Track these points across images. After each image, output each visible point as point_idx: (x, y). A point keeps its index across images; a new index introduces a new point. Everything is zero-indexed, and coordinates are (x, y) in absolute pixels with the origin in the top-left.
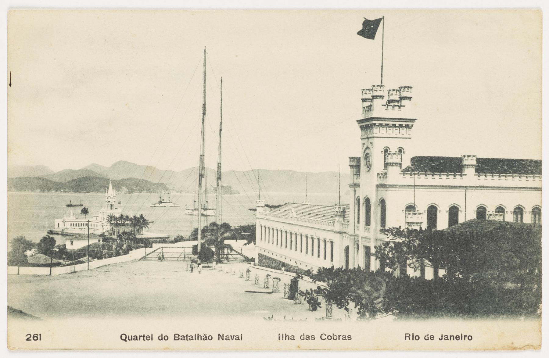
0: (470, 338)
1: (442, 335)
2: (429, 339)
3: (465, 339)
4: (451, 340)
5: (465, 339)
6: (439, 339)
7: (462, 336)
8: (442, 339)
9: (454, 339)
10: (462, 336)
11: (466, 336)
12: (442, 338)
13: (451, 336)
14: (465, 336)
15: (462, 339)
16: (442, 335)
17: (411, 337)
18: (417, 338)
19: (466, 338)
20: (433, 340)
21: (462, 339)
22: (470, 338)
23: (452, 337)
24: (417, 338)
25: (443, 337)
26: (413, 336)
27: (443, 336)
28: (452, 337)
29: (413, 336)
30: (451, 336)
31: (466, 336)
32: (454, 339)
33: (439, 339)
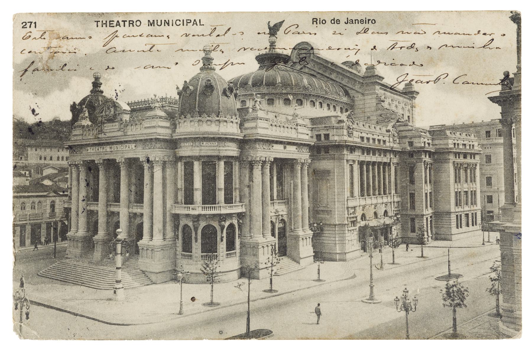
0: (373, 22)
1: (347, 18)
2: (335, 23)
3: (368, 23)
4: (355, 23)
5: (368, 23)
6: (345, 22)
7: (366, 20)
8: (348, 23)
9: (358, 23)
10: (366, 20)
11: (370, 20)
12: (348, 21)
13: (355, 20)
14: (369, 20)
15: (366, 23)
16: (347, 18)
17: (318, 22)
18: (324, 22)
19: (370, 22)
20: (339, 23)
21: (366, 23)
22: (373, 22)
23: (357, 21)
24: (324, 22)
25: (349, 21)
26: (320, 20)
27: (349, 19)
28: (357, 21)
29: (320, 20)
30: (355, 20)
31: (370, 20)
32: (358, 23)
33: (345, 22)
